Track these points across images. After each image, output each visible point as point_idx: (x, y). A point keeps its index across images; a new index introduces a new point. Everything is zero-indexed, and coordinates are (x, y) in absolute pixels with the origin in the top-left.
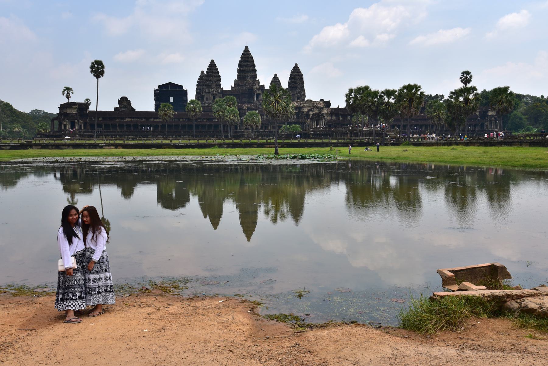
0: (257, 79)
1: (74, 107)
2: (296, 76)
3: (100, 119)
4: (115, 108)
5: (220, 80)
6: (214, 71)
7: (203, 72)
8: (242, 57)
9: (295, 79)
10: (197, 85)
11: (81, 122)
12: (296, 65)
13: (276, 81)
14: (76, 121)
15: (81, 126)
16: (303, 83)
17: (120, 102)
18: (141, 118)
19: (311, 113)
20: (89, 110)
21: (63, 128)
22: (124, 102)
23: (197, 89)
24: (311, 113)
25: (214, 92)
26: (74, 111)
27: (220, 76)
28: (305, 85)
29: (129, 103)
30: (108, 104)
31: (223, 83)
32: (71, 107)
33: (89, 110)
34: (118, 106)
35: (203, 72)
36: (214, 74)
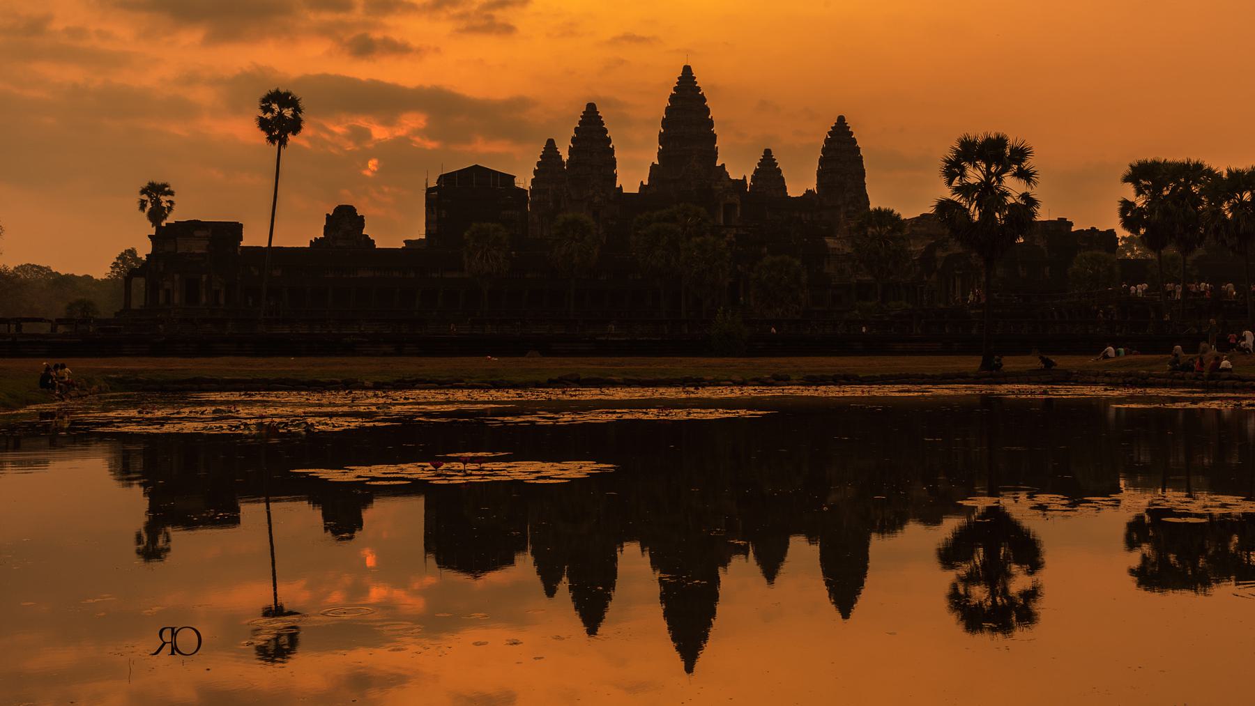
0: (718, 164)
1: (197, 233)
2: (841, 154)
4: (316, 243)
7: (551, 144)
8: (672, 98)
19: (939, 254)
20: (243, 244)
21: (162, 300)
22: (345, 220)
24: (939, 254)
25: (597, 199)
26: (198, 247)
29: (360, 221)
30: (300, 230)
31: (619, 171)
33: (243, 244)
35: (551, 144)
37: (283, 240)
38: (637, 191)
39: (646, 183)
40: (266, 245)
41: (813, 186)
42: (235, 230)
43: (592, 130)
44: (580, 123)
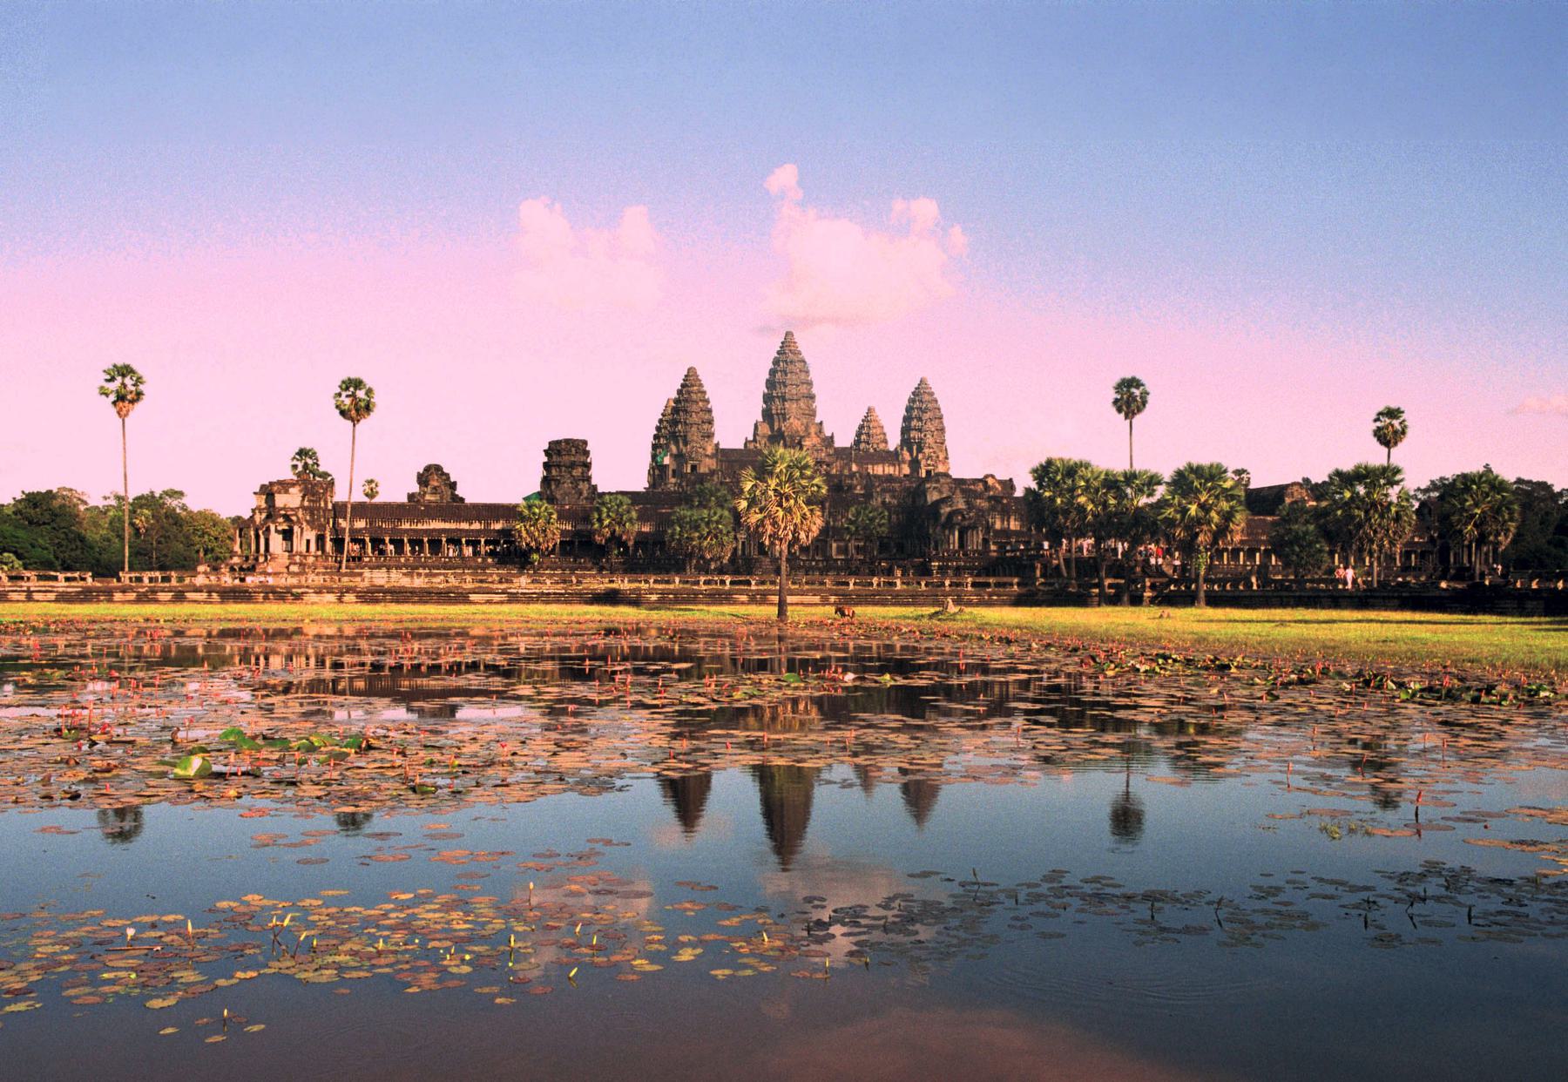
0: (817, 420)
1: (291, 490)
2: (921, 411)
4: (411, 497)
5: (710, 422)
6: (694, 397)
8: (776, 362)
9: (920, 419)
10: (656, 437)
11: (311, 535)
14: (296, 529)
16: (942, 430)
17: (423, 479)
18: (470, 520)
27: (710, 411)
28: (947, 436)
32: (287, 492)
34: (415, 488)
39: (751, 438)
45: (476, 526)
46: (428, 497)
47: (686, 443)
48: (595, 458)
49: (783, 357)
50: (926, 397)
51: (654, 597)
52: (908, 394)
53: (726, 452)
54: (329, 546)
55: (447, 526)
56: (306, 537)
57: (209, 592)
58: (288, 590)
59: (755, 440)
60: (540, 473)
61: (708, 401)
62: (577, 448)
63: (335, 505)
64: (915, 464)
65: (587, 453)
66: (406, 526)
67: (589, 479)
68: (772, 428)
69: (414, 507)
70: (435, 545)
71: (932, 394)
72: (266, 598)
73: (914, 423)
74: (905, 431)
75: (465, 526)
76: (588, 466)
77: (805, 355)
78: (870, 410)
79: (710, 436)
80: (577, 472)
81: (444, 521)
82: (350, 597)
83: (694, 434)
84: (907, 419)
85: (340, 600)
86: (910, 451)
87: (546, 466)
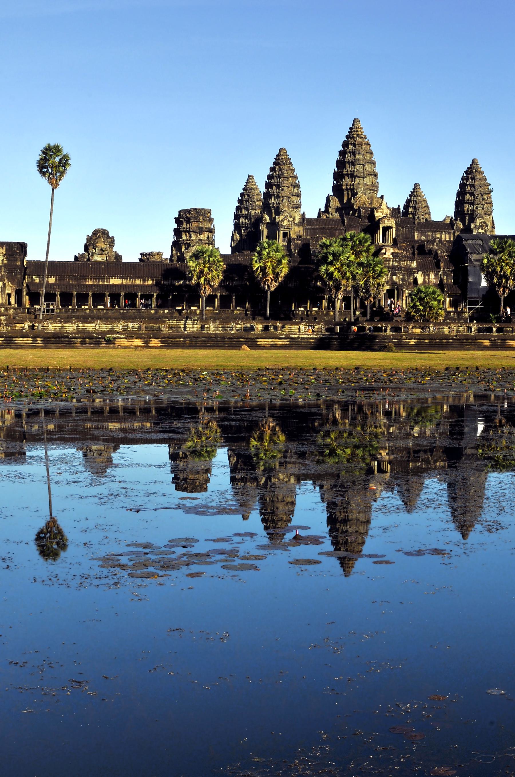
0: (379, 195)
3: (52, 280)
5: (298, 195)
8: (345, 145)
9: (472, 194)
10: (238, 208)
12: (473, 161)
13: (415, 200)
15: (9, 295)
16: (491, 203)
20: (27, 258)
23: (237, 217)
25: (286, 223)
27: (297, 186)
29: (111, 242)
30: (67, 248)
36: (286, 182)
37: (56, 256)
38: (316, 217)
39: (323, 210)
40: (43, 259)
41: (451, 211)
42: (22, 247)
43: (280, 170)
44: (274, 163)
45: (150, 282)
46: (97, 258)
47: (278, 213)
48: (217, 225)
49: (351, 141)
50: (479, 176)
51: (412, 342)
52: (461, 173)
53: (310, 221)
54: (26, 300)
55: (124, 282)
56: (8, 291)
57: (35, 338)
58: (103, 334)
59: (327, 211)
60: (171, 238)
61: (296, 177)
62: (205, 215)
63: (29, 262)
64: (467, 230)
65: (211, 220)
66: (90, 283)
67: (211, 242)
68: (341, 200)
69: (81, 265)
70: (131, 297)
71: (482, 173)
72: (83, 343)
73: (468, 197)
74: (459, 204)
75: (138, 282)
76: (211, 231)
77: (370, 139)
78: (416, 186)
79: (298, 206)
80: (204, 237)
81: (122, 278)
82: (155, 342)
83: (285, 206)
84: (461, 194)
85: (147, 346)
86: (463, 221)
87: (177, 232)
